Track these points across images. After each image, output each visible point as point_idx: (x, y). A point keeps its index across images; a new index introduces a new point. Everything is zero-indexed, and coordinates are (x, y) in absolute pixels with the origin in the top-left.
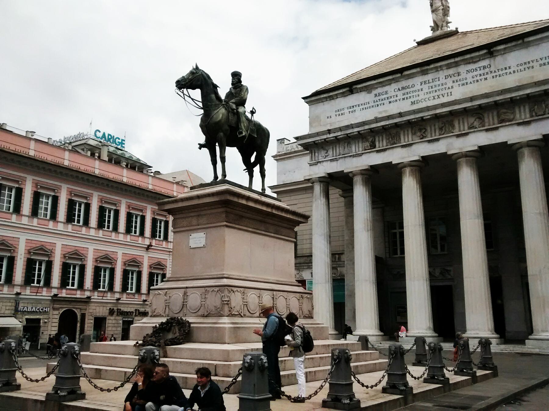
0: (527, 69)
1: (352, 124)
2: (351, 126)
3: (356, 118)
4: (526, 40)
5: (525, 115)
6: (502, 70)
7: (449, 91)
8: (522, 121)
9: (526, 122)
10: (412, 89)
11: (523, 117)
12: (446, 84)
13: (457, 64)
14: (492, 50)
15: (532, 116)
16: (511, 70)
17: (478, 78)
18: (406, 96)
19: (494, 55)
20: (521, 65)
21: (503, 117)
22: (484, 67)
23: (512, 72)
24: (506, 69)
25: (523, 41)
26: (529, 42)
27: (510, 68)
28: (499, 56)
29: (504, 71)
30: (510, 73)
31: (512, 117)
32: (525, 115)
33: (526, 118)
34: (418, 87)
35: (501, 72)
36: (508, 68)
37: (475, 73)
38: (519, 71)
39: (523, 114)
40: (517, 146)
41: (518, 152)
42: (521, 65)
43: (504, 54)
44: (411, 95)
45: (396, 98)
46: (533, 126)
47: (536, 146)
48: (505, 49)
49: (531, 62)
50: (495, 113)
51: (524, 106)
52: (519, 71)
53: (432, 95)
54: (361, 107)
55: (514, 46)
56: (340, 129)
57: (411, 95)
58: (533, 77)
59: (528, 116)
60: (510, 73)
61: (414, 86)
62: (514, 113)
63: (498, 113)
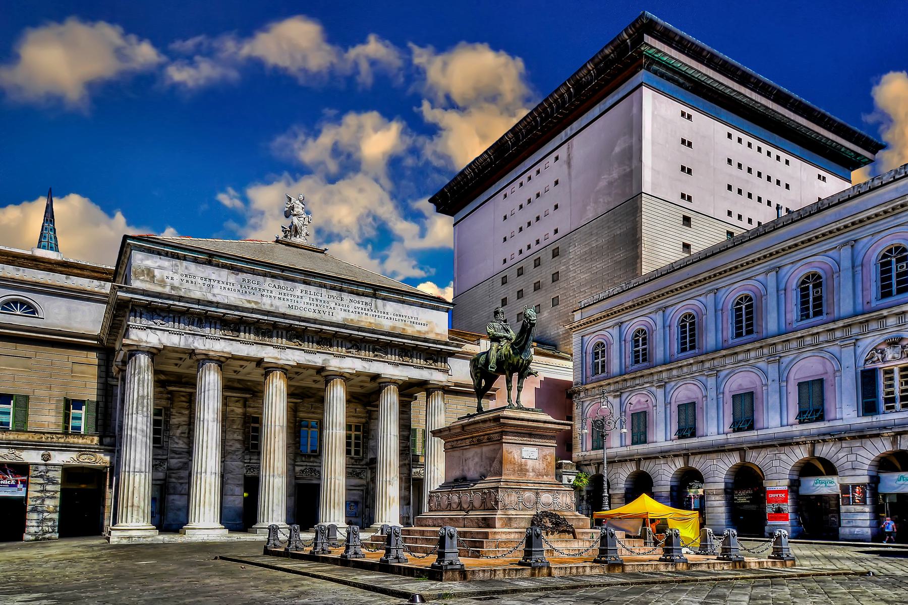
1: (218, 303)
2: (218, 305)
3: (214, 295)
7: (331, 311)
10: (290, 293)
12: (328, 302)
13: (341, 290)
17: (360, 310)
18: (282, 297)
22: (366, 304)
34: (298, 293)
37: (357, 305)
44: (289, 298)
45: (269, 294)
53: (312, 307)
54: (224, 285)
56: (198, 302)
57: (289, 298)
61: (292, 289)
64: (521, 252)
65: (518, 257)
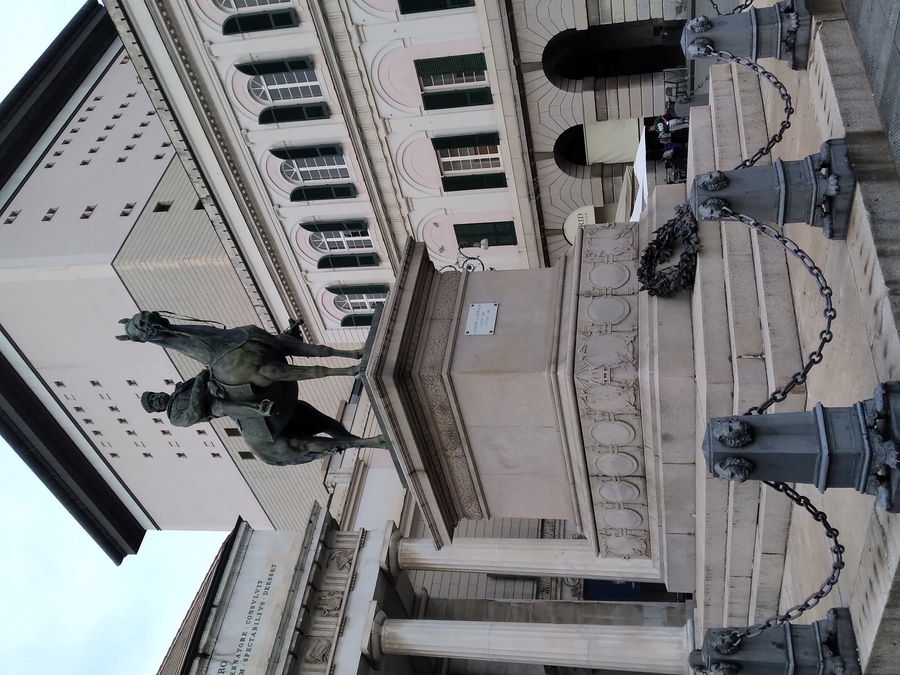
0: (260, 612)
8: (338, 628)
11: (333, 626)
14: (201, 652)
15: (337, 616)
19: (210, 653)
20: (249, 618)
21: (319, 654)
24: (243, 640)
26: (221, 602)
27: (244, 634)
29: (246, 643)
31: (324, 643)
32: (331, 623)
35: (245, 647)
36: (244, 637)
39: (327, 626)
40: (375, 639)
42: (249, 618)
46: (351, 614)
50: (307, 666)
51: (316, 622)
59: (334, 619)
62: (319, 639)
63: (307, 661)
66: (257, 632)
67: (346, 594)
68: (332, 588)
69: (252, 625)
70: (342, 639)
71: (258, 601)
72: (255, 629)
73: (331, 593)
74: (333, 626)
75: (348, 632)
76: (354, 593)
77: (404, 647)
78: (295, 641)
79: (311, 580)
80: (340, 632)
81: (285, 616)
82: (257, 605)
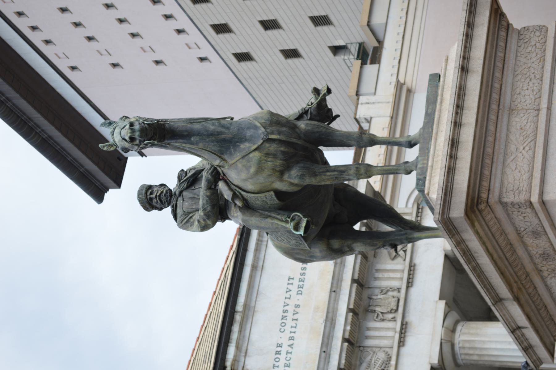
0: (296, 317)
4: (240, 307)
5: (388, 329)
6: (277, 360)
8: (397, 336)
9: (402, 329)
11: (390, 333)
15: (394, 319)
16: (286, 343)
20: (283, 325)
23: (291, 342)
24: (278, 353)
25: (240, 312)
26: (246, 306)
27: (279, 346)
28: (246, 363)
29: (283, 356)
30: (291, 346)
31: (381, 356)
32: (388, 329)
33: (394, 329)
36: (279, 349)
38: (293, 330)
40: (447, 349)
41: (460, 362)
42: (283, 325)
43: (246, 353)
46: (412, 318)
47: (457, 323)
48: (238, 348)
49: (286, 308)
51: (368, 329)
52: (293, 330)
55: (240, 331)
58: (317, 309)
59: (390, 325)
60: (291, 346)
64: (179, 32)
65: (193, 35)
66: (295, 342)
67: (403, 291)
68: (385, 284)
69: (287, 334)
70: (404, 350)
71: (292, 303)
72: (292, 338)
73: (385, 291)
74: (390, 333)
75: (410, 340)
76: (413, 291)
77: (486, 358)
78: (344, 355)
79: (356, 277)
80: (400, 342)
81: (328, 324)
82: (290, 309)
